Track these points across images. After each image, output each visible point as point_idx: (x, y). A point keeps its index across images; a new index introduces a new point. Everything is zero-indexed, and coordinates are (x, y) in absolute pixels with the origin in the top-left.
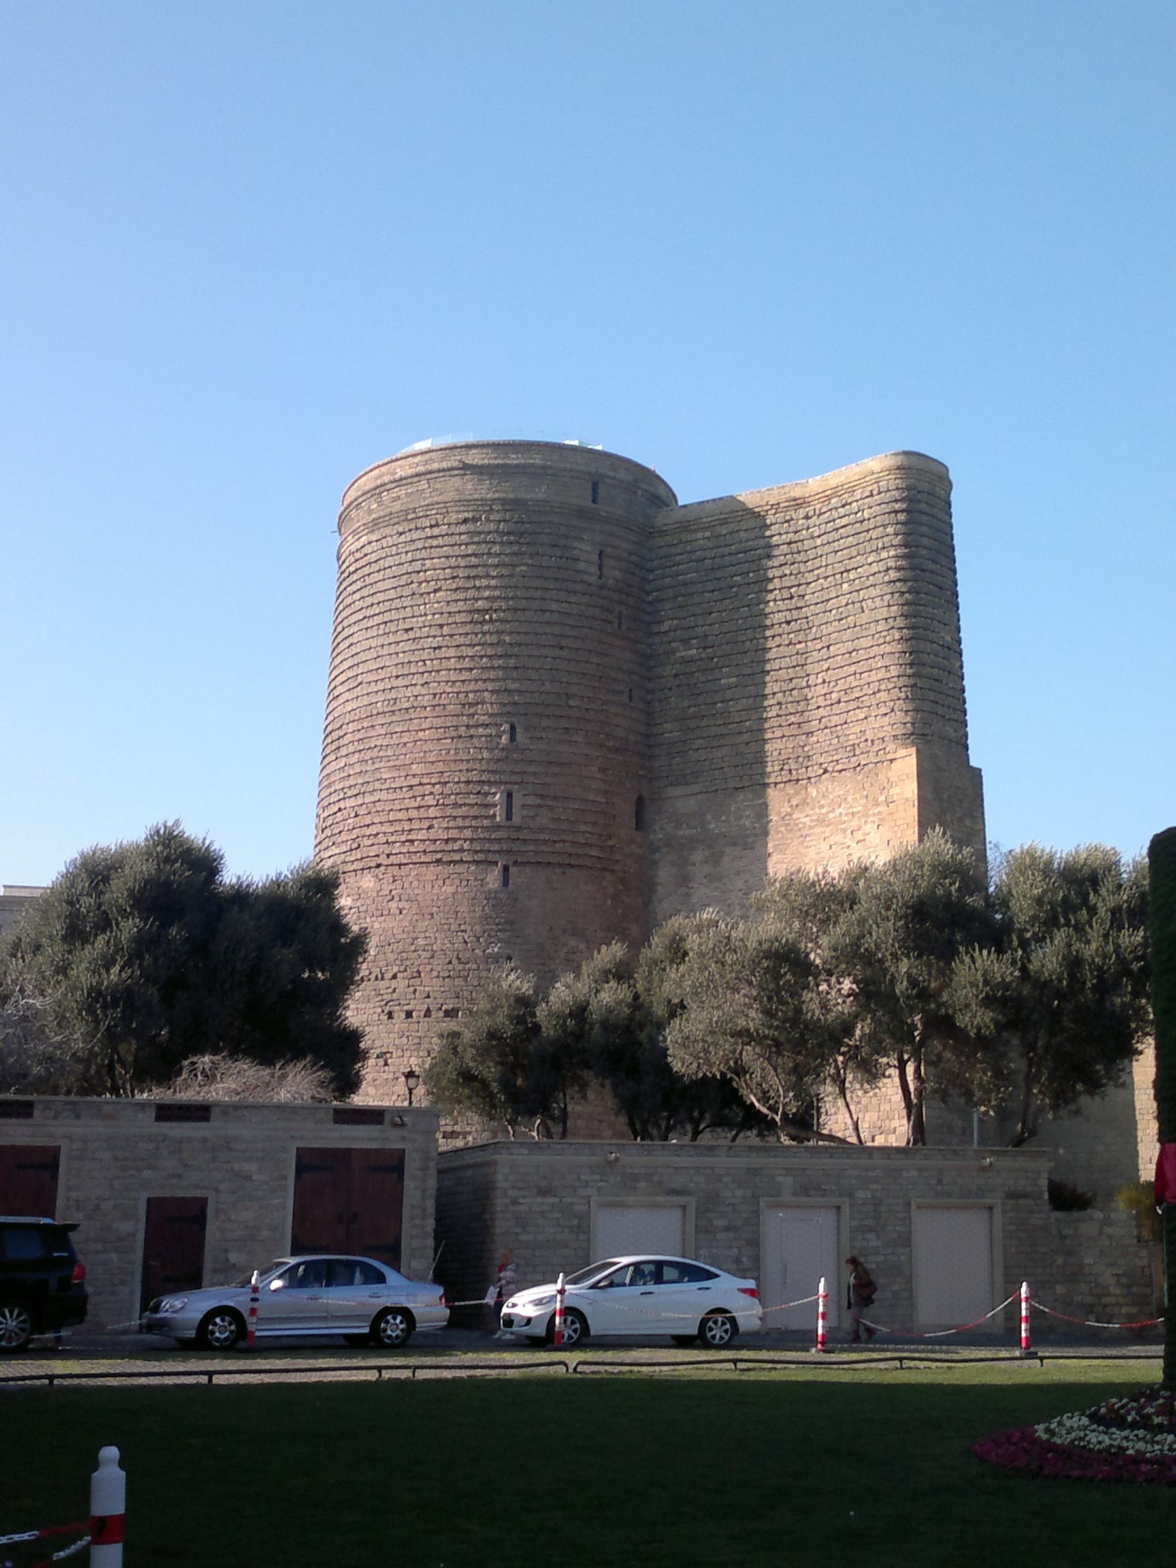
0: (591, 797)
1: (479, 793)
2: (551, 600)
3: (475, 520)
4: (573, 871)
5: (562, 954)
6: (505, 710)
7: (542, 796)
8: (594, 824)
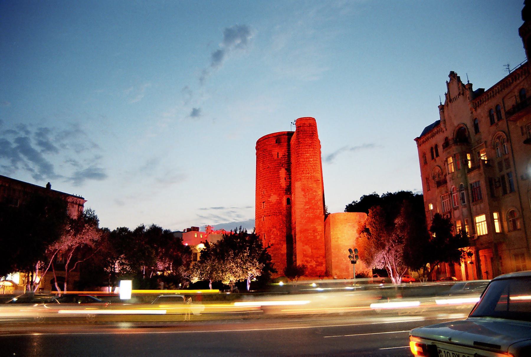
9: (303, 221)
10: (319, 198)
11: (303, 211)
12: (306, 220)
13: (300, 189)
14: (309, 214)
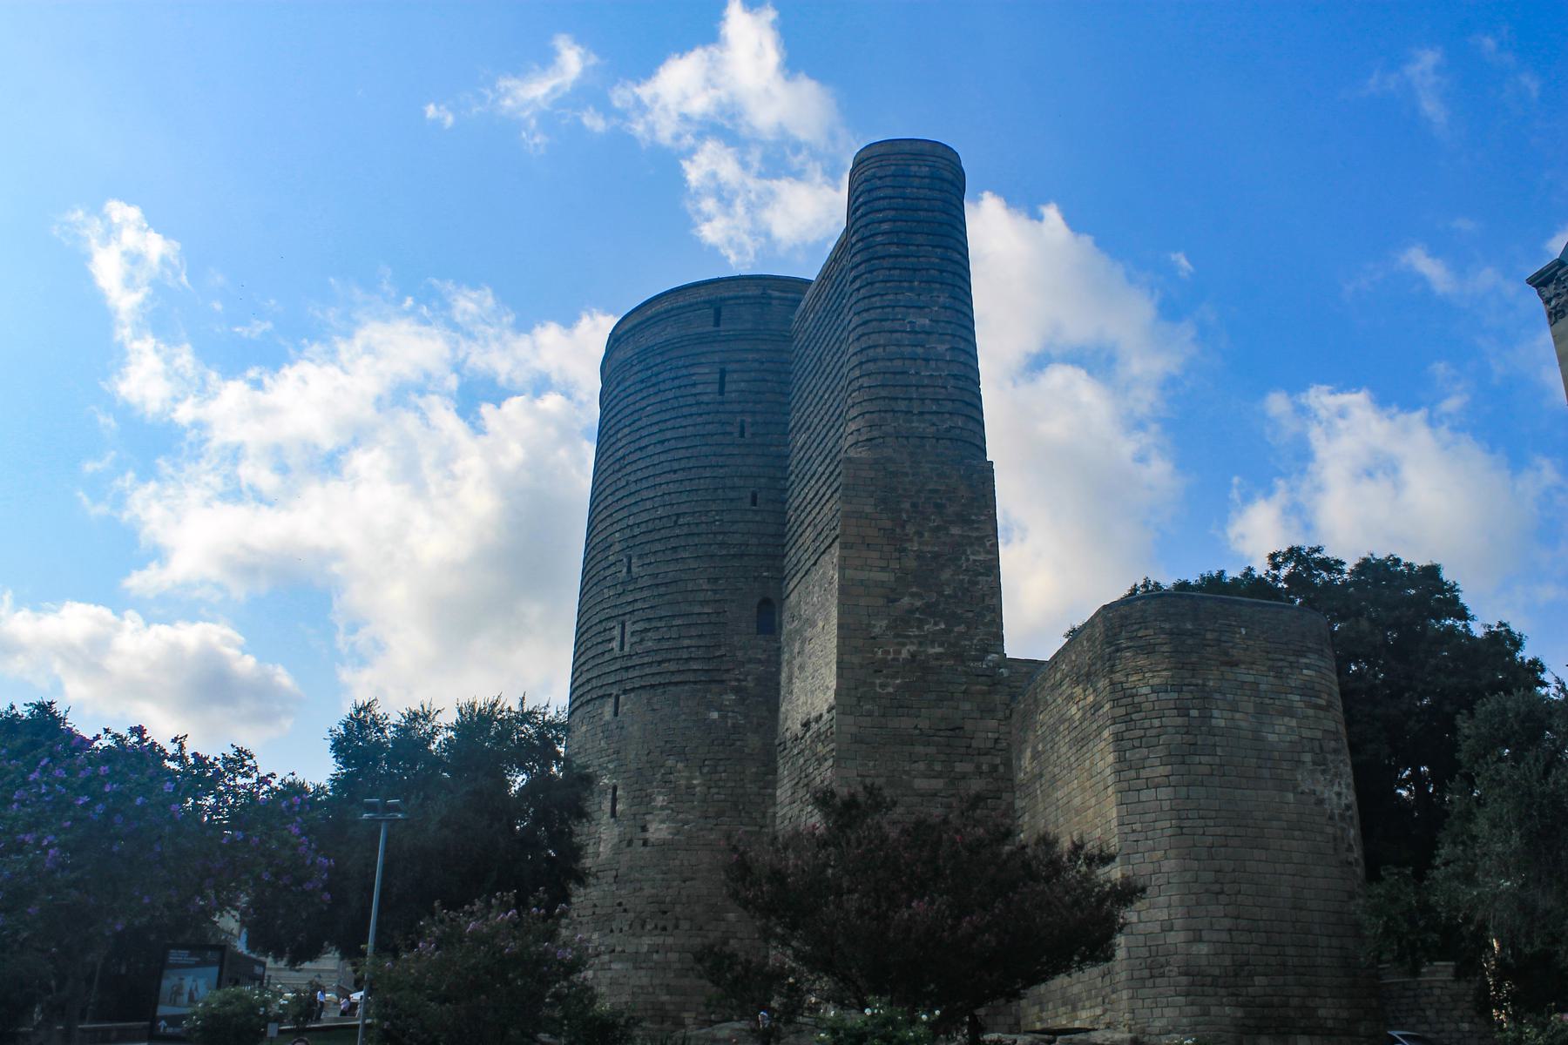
0: (697, 609)
1: (605, 630)
2: (667, 429)
3: (624, 380)
4: (672, 688)
5: (658, 776)
6: (625, 545)
7: (649, 620)
8: (700, 636)
9: (883, 686)
11: (884, 623)
12: (898, 681)
13: (872, 501)
14: (920, 644)
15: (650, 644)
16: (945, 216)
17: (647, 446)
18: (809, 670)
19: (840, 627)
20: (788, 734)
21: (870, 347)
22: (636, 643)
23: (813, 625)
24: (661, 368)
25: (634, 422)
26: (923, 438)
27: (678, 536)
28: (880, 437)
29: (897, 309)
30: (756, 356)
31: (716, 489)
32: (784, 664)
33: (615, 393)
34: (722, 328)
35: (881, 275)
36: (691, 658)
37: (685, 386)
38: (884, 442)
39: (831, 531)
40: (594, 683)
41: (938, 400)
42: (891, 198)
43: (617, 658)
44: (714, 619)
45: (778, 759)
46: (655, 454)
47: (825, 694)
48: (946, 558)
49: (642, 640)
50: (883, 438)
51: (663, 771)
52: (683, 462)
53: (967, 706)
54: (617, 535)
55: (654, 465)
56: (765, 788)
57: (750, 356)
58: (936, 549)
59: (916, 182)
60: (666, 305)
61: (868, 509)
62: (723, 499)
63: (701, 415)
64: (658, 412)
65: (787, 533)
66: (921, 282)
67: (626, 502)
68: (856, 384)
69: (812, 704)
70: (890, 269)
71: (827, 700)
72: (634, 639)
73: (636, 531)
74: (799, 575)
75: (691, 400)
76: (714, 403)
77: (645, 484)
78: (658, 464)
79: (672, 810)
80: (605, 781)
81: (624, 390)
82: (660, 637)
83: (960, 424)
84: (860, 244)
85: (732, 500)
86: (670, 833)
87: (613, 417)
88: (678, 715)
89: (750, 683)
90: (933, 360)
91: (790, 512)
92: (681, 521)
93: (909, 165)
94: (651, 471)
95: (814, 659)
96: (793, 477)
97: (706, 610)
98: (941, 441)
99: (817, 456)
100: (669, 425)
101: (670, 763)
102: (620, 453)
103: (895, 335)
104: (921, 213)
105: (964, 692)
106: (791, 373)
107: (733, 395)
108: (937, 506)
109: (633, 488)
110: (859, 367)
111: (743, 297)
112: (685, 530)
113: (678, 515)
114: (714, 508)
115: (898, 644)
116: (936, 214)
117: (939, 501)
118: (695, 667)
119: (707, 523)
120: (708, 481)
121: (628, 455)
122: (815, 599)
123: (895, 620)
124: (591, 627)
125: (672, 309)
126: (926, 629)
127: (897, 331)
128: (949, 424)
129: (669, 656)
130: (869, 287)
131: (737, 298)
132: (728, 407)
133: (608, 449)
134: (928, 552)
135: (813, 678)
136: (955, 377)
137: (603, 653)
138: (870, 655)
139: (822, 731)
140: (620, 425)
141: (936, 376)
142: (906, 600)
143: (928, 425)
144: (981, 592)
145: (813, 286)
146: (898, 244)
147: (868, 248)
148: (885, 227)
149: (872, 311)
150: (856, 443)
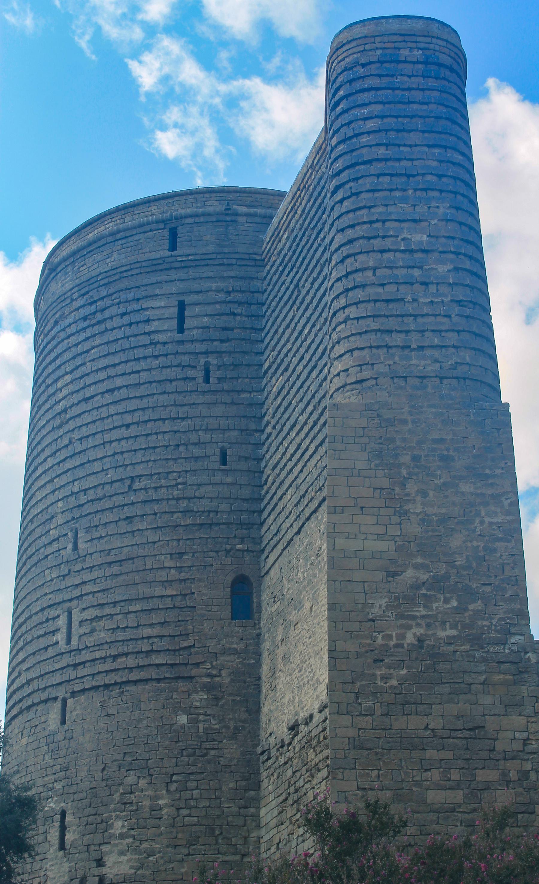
0: (158, 591)
1: (47, 620)
2: (117, 376)
3: (63, 317)
4: (131, 688)
5: (116, 797)
6: (69, 516)
8: (162, 624)
9: (385, 678)
10: (499, 519)
12: (404, 672)
13: (364, 455)
14: (428, 625)
15: (103, 635)
16: (441, 108)
17: (92, 397)
18: (296, 661)
19: (331, 608)
20: (272, 740)
21: (356, 271)
22: (85, 634)
23: (299, 606)
24: (108, 302)
25: (77, 368)
26: (424, 377)
27: (133, 504)
28: (372, 378)
29: (388, 224)
30: (221, 285)
31: (178, 446)
32: (265, 655)
33: (52, 333)
34: (178, 252)
35: (367, 183)
36: (152, 651)
37: (137, 323)
38: (377, 385)
39: (317, 492)
40: (35, 685)
41: (440, 331)
42: (377, 89)
43: (62, 654)
44: (178, 602)
45: (262, 770)
46: (102, 406)
47: (315, 689)
48: (456, 520)
49: (92, 631)
50: (376, 379)
51: (121, 791)
52: (136, 414)
53: (487, 700)
54: (60, 504)
55: (103, 419)
56: (246, 807)
57: (214, 286)
58: (444, 510)
59: (407, 68)
60: (111, 226)
61: (360, 465)
62: (185, 458)
63: (156, 357)
64: (105, 356)
65: (264, 496)
66: (415, 190)
67: (69, 464)
68: (341, 316)
69: (300, 702)
70: (378, 176)
71: (318, 697)
72: (82, 631)
73: (83, 499)
74: (280, 547)
75: (146, 340)
76: (172, 342)
77: (91, 442)
78: (107, 418)
79: (134, 837)
80: (52, 805)
81: (63, 330)
82: (115, 627)
83: (468, 360)
84: (341, 147)
85: (196, 459)
86: (131, 867)
87: (50, 363)
88: (138, 721)
89: (225, 679)
90: (432, 283)
91: (267, 471)
92: (137, 485)
93: (399, 49)
94: (98, 427)
95: (301, 647)
96: (269, 429)
97: (169, 592)
98: (445, 381)
99: (298, 403)
100: (120, 369)
101: (130, 780)
102: (61, 406)
103: (386, 256)
104: (415, 107)
105: (483, 684)
106: (263, 304)
107: (195, 332)
108: (442, 458)
109: (78, 447)
110: (344, 295)
111: (204, 215)
112: (142, 496)
113: (132, 478)
114: (175, 469)
115: (402, 626)
116: (432, 107)
117: (446, 453)
118: (157, 662)
119: (167, 487)
120: (167, 436)
121: (71, 407)
122: (300, 575)
123: (397, 598)
124: (30, 617)
125: (119, 231)
126: (434, 608)
127: (389, 250)
128: (455, 359)
129: (126, 649)
130: (354, 198)
131: (196, 215)
132: (188, 347)
133: (46, 401)
134: (434, 514)
135: (300, 671)
136: (459, 302)
137: (46, 648)
138: (368, 641)
139: (313, 734)
140: (59, 373)
141: (437, 302)
142: (410, 573)
143: (429, 362)
144: (501, 561)
145: (287, 199)
146: (387, 145)
147: (352, 151)
148: (371, 125)
149: (358, 228)
150: (344, 386)
